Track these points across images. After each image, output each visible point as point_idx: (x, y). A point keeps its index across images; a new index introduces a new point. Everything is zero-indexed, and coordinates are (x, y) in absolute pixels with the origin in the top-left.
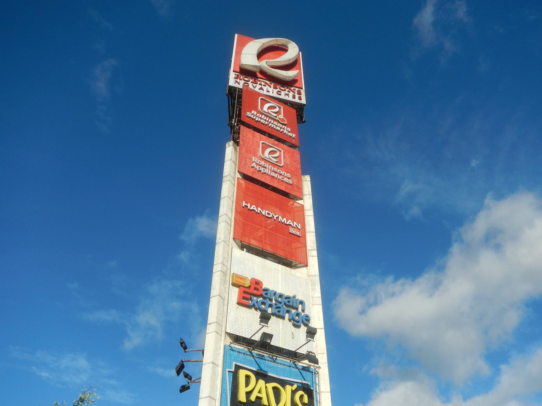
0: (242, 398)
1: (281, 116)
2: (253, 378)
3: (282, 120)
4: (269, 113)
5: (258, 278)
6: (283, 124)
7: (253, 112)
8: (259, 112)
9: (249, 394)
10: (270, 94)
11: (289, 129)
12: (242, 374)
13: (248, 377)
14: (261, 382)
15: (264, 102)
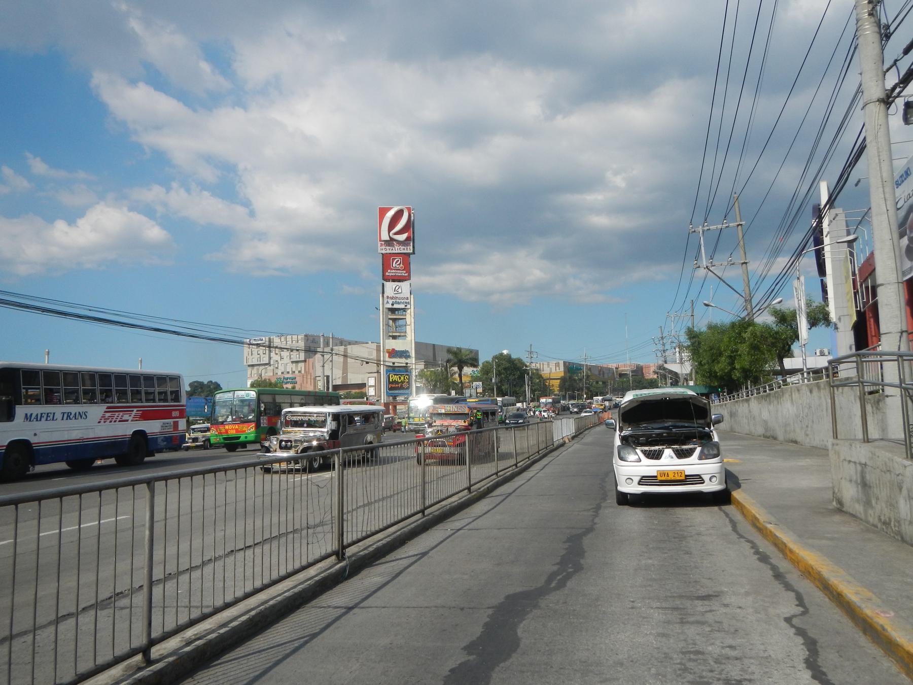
0: (391, 381)
1: (401, 265)
2: (393, 375)
3: (402, 267)
4: (396, 267)
5: (393, 348)
6: (402, 270)
7: (389, 271)
8: (391, 269)
9: (392, 380)
10: (396, 252)
11: (405, 272)
12: (391, 375)
13: (392, 376)
14: (396, 376)
15: (393, 260)
